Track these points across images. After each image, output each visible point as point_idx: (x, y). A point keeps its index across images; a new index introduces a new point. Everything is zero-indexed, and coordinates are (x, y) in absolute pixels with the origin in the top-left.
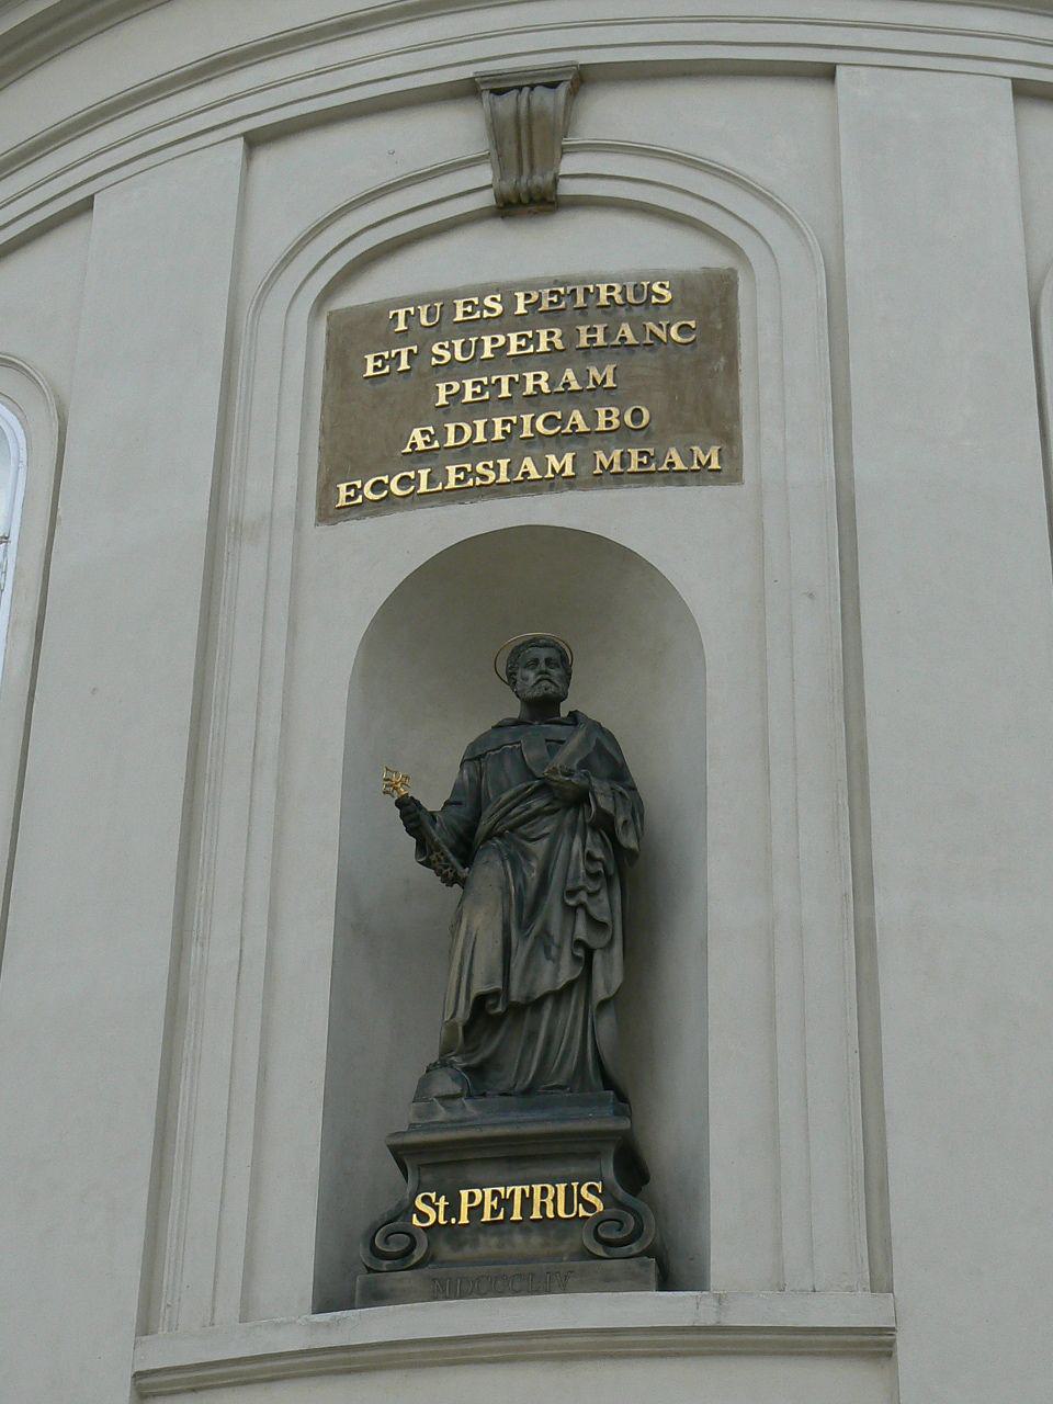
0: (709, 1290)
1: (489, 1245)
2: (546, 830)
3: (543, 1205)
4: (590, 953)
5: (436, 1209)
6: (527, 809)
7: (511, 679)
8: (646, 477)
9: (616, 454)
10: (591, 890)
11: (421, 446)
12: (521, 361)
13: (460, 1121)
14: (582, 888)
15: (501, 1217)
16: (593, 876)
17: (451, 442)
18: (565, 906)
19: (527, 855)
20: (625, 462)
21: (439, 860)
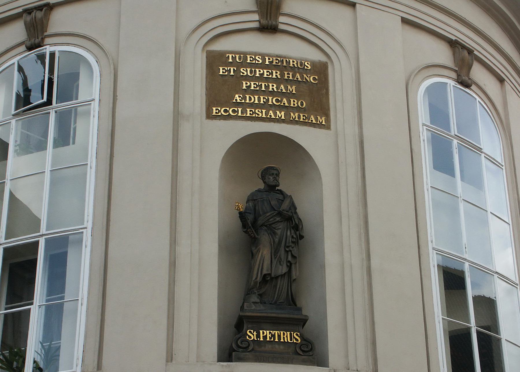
0: (328, 367)
1: (269, 347)
2: (280, 227)
3: (284, 338)
4: (291, 264)
5: (253, 335)
6: (275, 220)
7: (263, 178)
8: (304, 123)
9: (297, 114)
10: (292, 246)
11: (239, 101)
12: (267, 80)
13: (259, 310)
14: (290, 246)
15: (272, 340)
16: (293, 242)
17: (248, 101)
18: (285, 250)
19: (275, 233)
20: (299, 117)
21: (250, 232)
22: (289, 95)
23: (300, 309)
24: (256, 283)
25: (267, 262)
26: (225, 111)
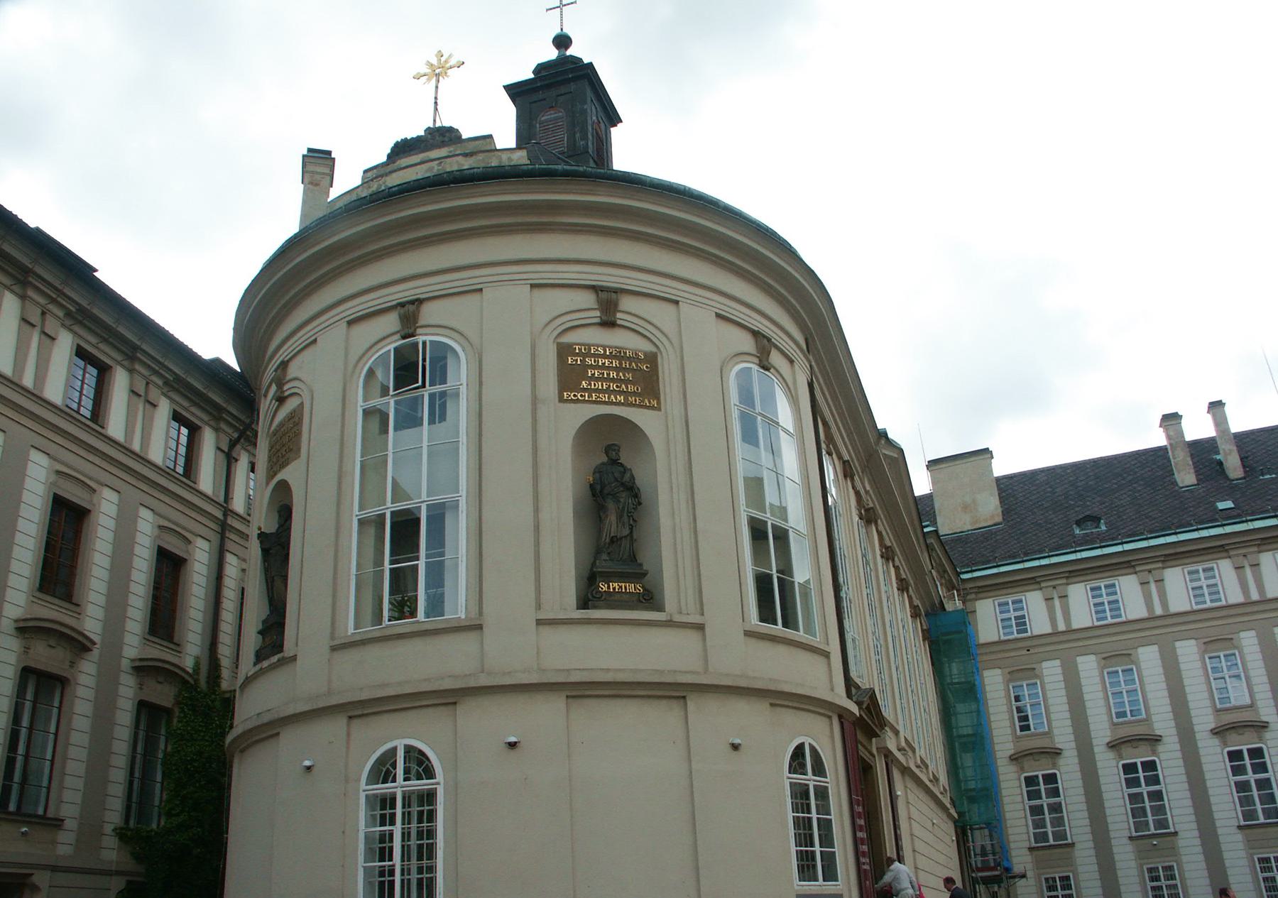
0: (665, 611)
1: (617, 597)
4: (632, 527)
7: (607, 453)
8: (640, 406)
9: (633, 398)
11: (585, 387)
12: (608, 368)
16: (634, 508)
17: (593, 387)
19: (620, 502)
20: (636, 401)
22: (627, 382)
23: (641, 565)
24: (605, 544)
25: (614, 526)
26: (575, 396)
